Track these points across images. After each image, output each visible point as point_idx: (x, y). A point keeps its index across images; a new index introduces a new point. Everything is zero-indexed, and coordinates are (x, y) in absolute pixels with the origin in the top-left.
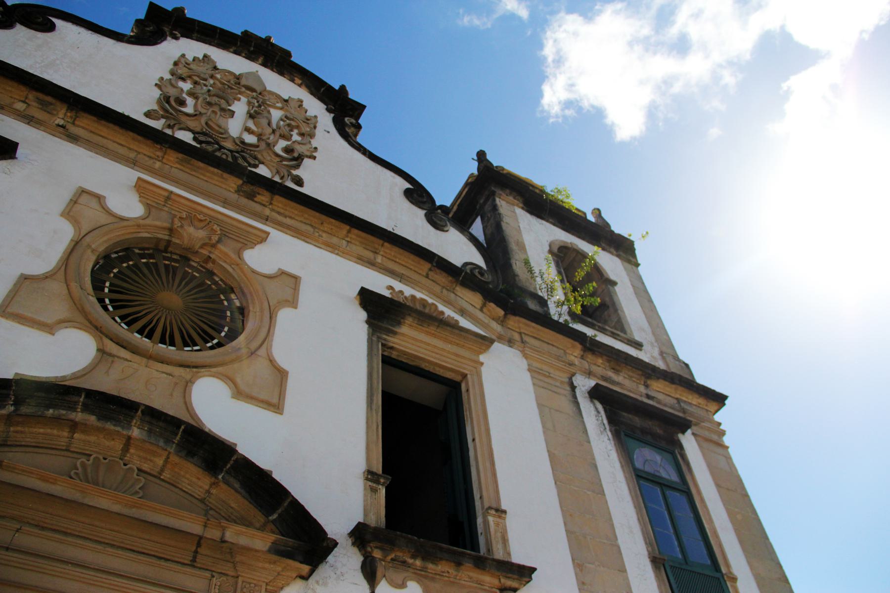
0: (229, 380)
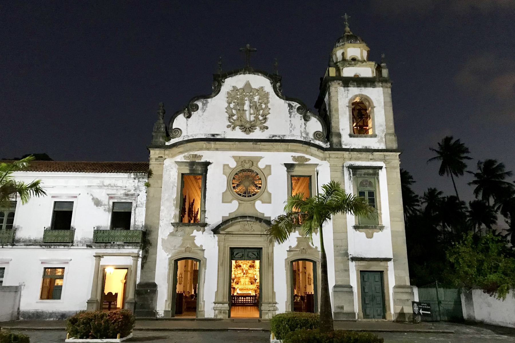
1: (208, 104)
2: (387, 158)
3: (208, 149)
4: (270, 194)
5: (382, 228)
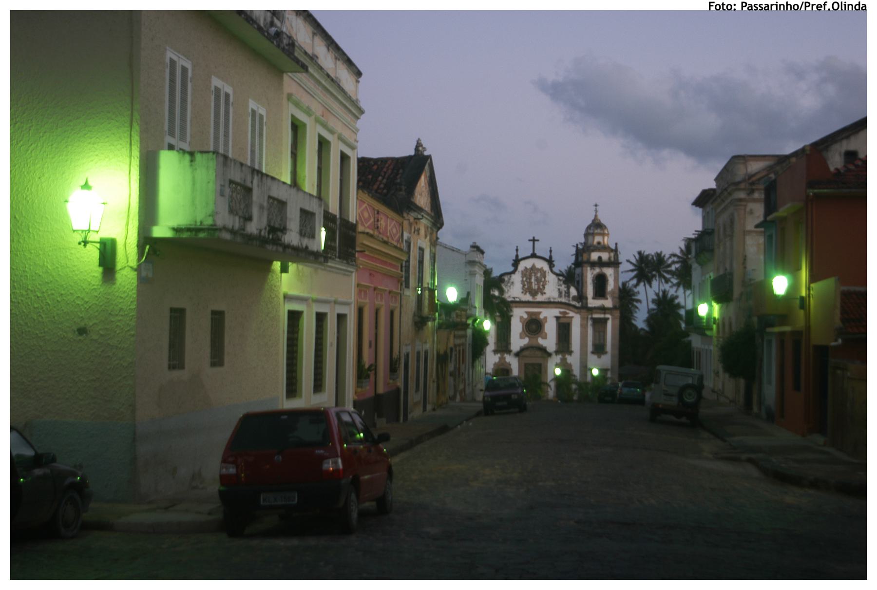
5: (606, 353)
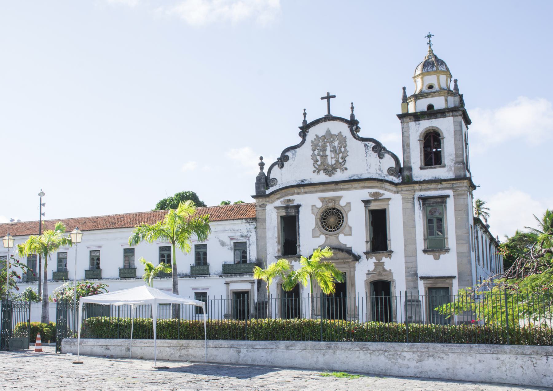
0: (343, 233)
1: (297, 154)
2: (455, 186)
3: (298, 193)
4: (350, 228)
5: (448, 250)
